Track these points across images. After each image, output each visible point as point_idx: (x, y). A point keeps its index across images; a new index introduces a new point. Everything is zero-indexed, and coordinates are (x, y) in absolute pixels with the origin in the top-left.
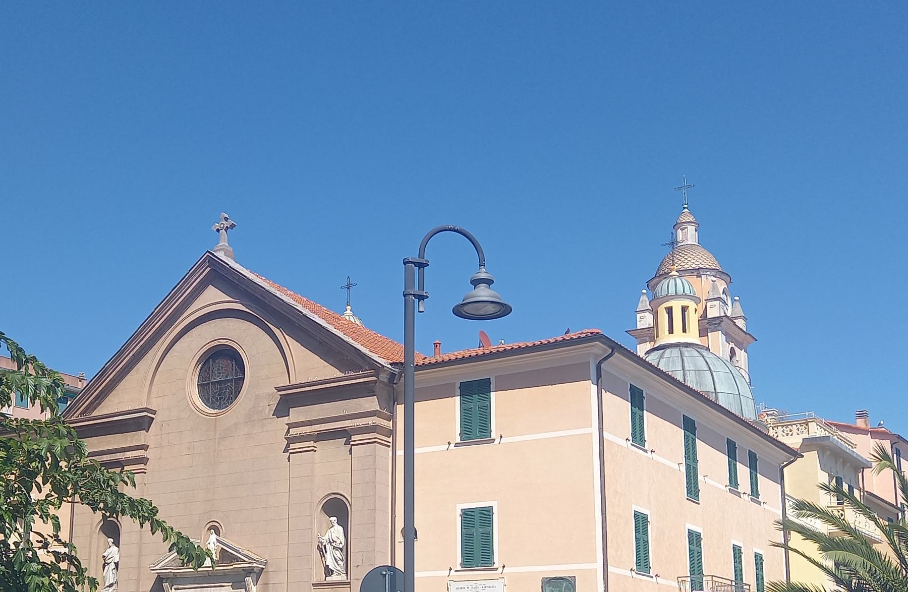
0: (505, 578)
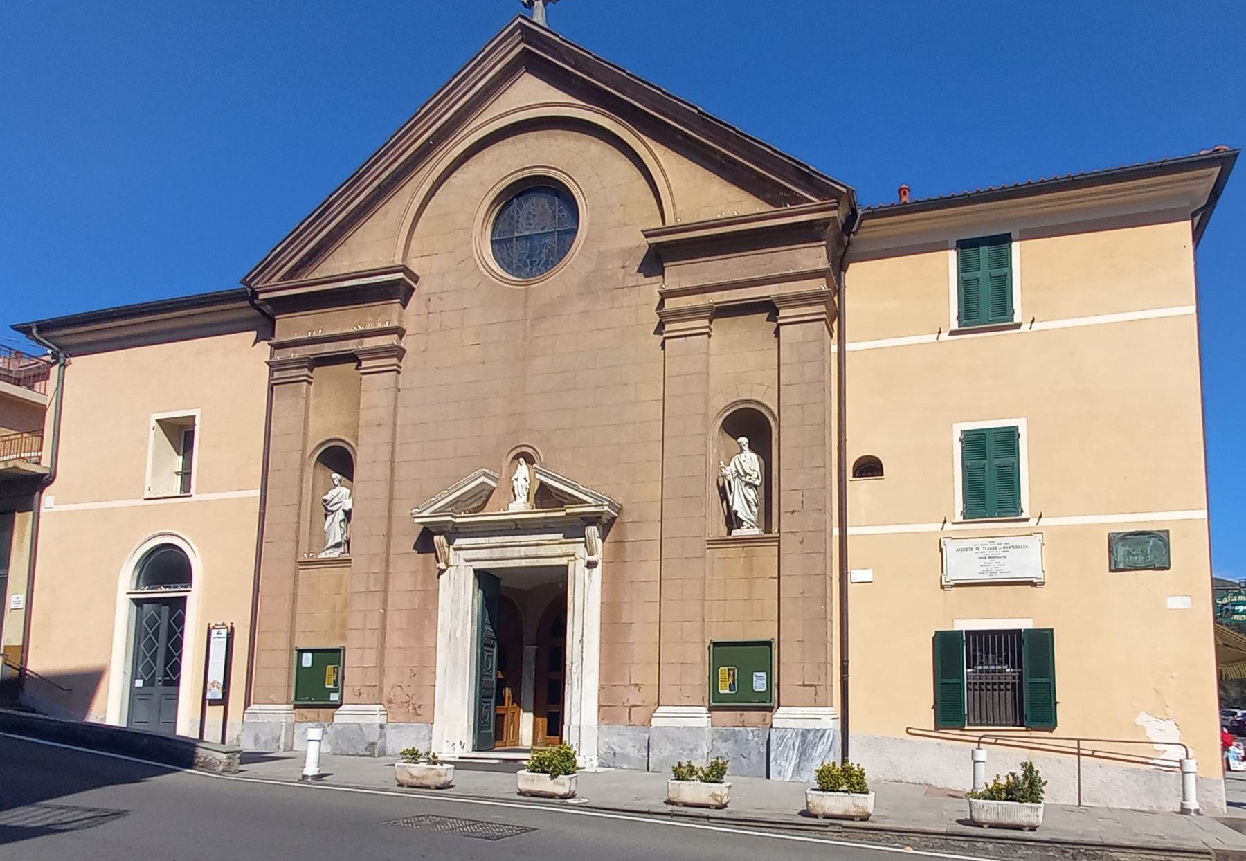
0: (1044, 534)
